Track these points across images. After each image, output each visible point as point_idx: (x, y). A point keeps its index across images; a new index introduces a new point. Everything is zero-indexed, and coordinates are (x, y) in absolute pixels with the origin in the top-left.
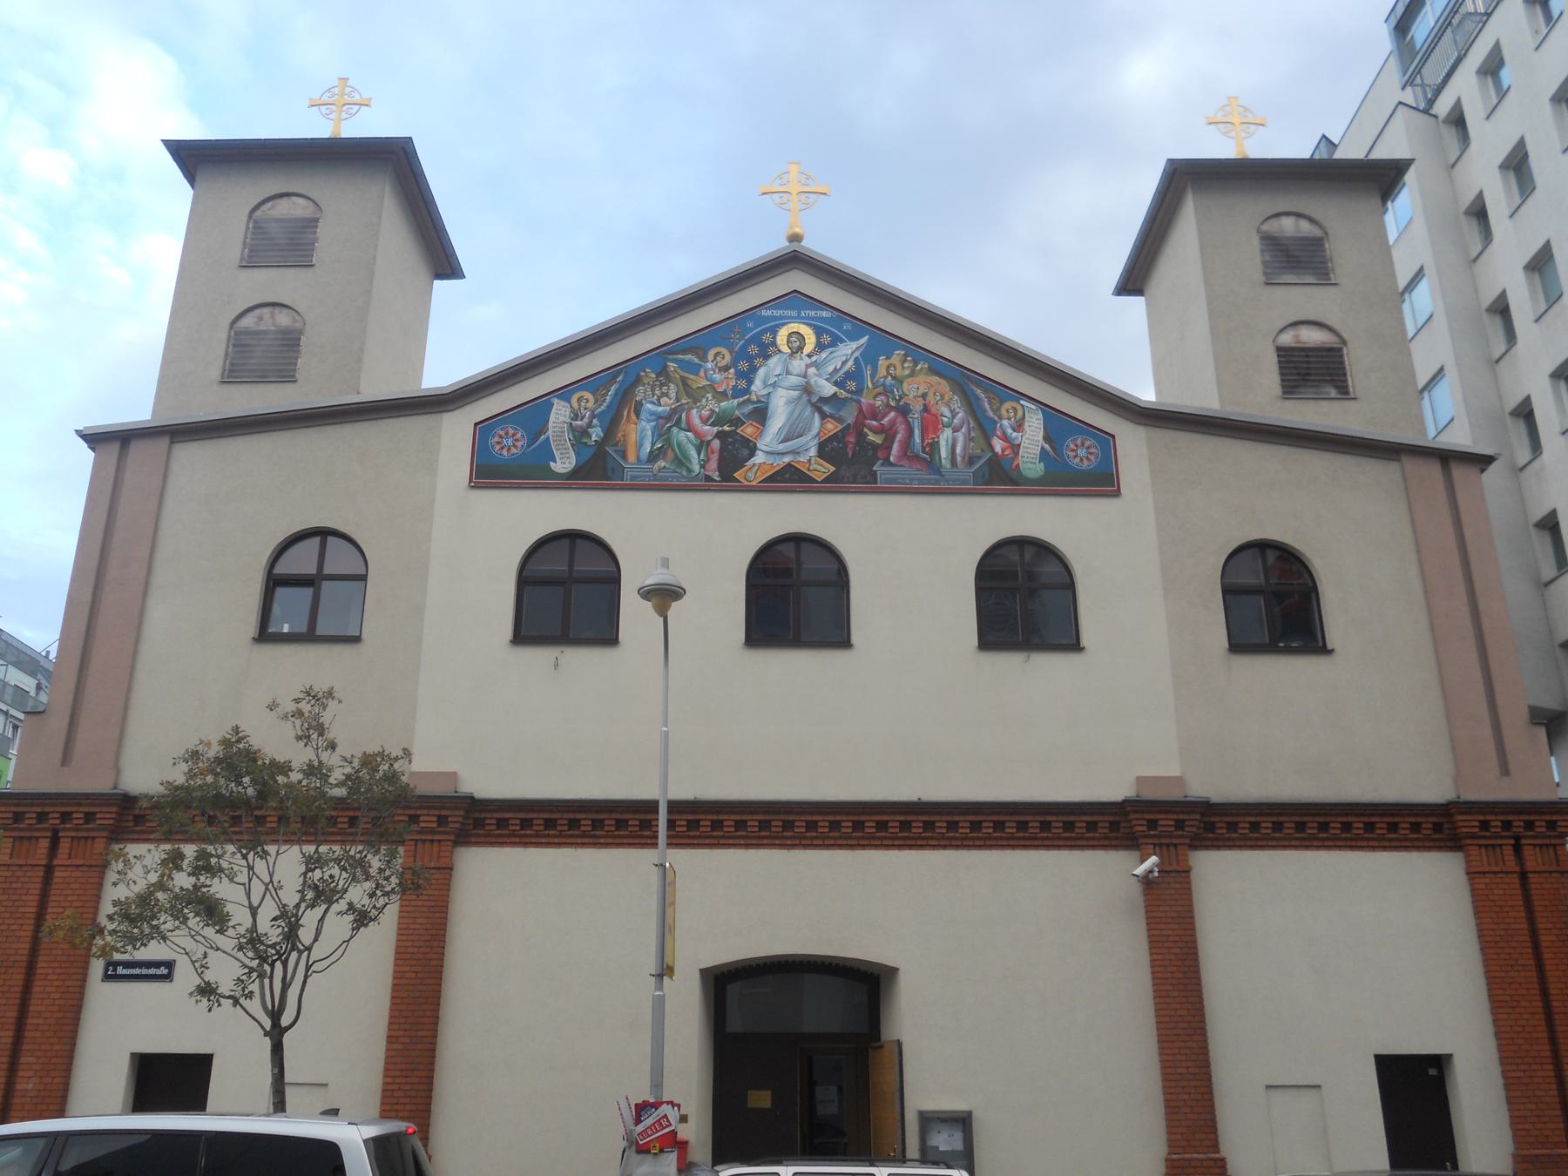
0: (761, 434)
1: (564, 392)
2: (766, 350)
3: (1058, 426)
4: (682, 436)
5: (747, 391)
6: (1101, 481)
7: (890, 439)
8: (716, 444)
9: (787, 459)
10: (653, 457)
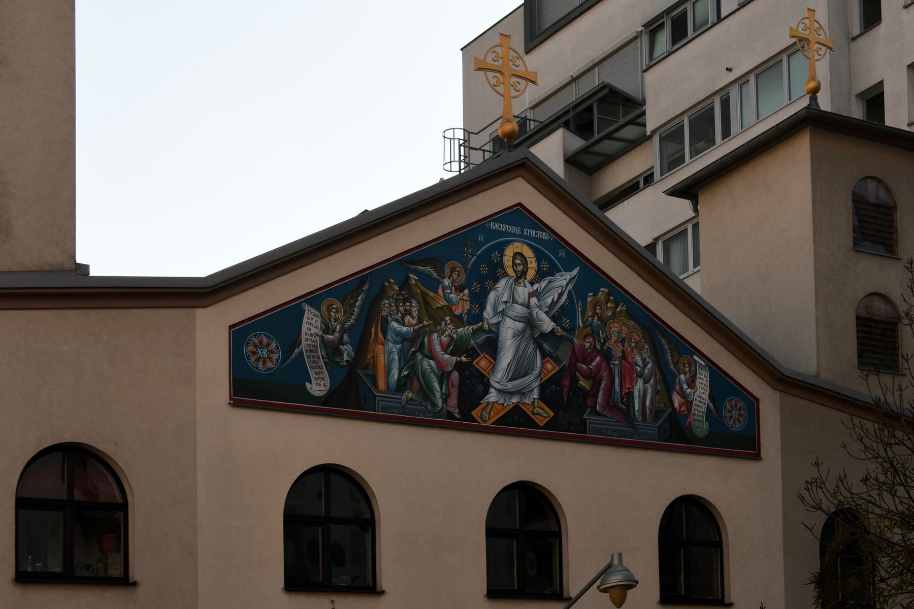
0: (493, 369)
1: (315, 298)
2: (495, 273)
3: (722, 384)
4: (428, 364)
5: (479, 318)
6: (746, 445)
7: (596, 386)
8: (455, 375)
9: (515, 400)
10: (403, 384)
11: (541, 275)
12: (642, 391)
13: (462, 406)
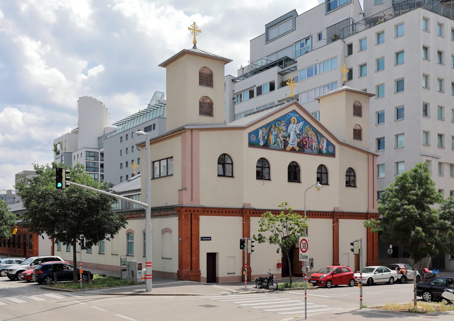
1: (261, 128)
3: (329, 143)
5: (287, 131)
6: (333, 155)
7: (306, 143)
9: (293, 146)
10: (275, 143)
11: (298, 123)
12: (315, 144)
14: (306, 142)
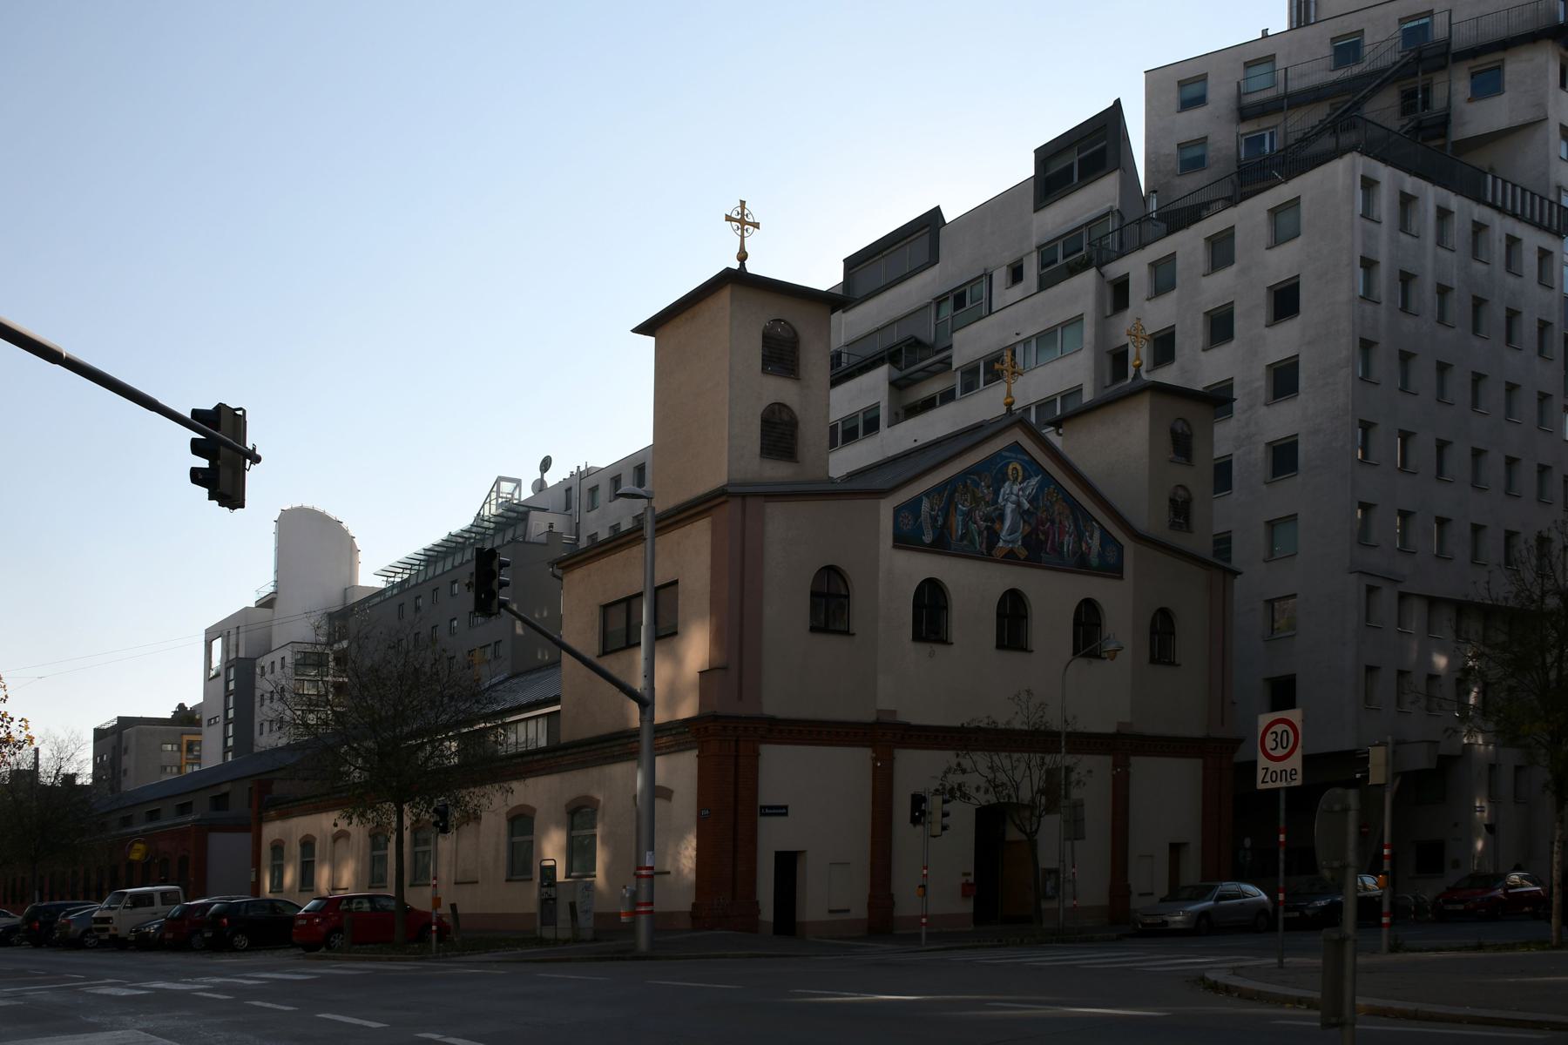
1: (927, 493)
3: (1106, 537)
5: (996, 502)
10: (963, 537)
12: (1068, 542)
13: (987, 550)
14: (1046, 534)
